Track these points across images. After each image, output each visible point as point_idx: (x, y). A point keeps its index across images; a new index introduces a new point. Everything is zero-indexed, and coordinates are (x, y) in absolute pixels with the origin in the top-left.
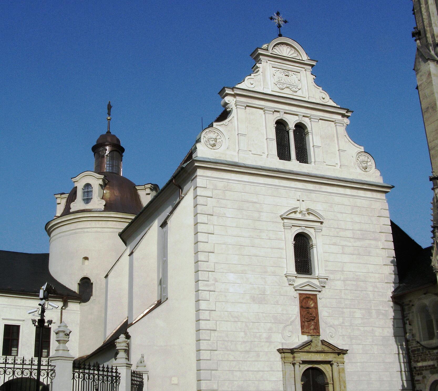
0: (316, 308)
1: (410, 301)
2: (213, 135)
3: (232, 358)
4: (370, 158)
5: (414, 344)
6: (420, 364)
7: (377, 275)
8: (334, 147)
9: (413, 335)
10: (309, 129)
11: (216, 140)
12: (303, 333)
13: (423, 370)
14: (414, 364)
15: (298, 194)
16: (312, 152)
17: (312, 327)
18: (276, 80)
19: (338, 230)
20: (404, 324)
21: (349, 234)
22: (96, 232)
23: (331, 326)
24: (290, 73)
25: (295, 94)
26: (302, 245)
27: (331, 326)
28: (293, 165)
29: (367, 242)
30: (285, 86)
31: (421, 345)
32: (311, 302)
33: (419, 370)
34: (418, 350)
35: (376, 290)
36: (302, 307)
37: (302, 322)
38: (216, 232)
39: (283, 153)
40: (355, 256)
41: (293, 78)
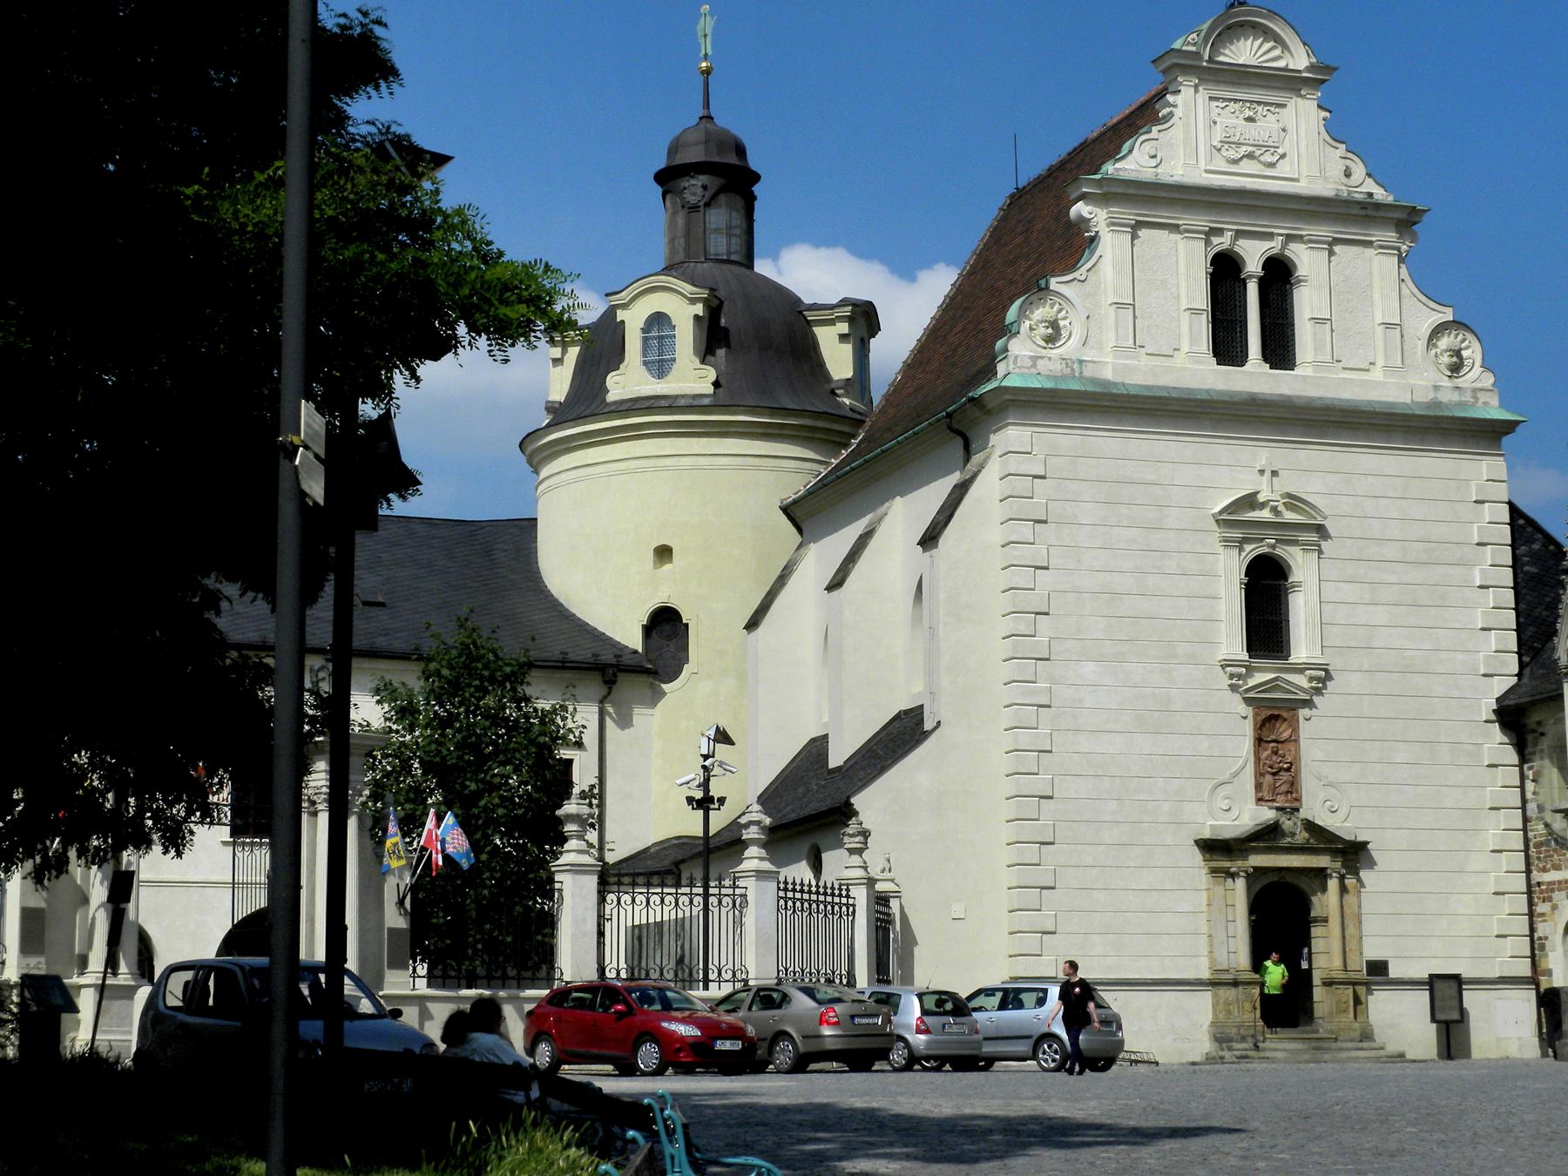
1: (1539, 723)
3: (1089, 861)
4: (1469, 336)
7: (1460, 656)
8: (1366, 323)
9: (1541, 808)
10: (1302, 270)
11: (1054, 324)
12: (1259, 800)
13: (1553, 890)
14: (1537, 876)
17: (1284, 788)
18: (1218, 134)
19: (1362, 543)
20: (1523, 777)
21: (1390, 551)
22: (694, 468)
25: (1269, 172)
27: (1330, 785)
28: (1254, 376)
30: (1243, 150)
32: (1285, 725)
33: (1547, 891)
35: (1456, 693)
36: (1259, 741)
37: (1259, 775)
38: (1053, 562)
39: (1227, 348)
41: (1268, 124)
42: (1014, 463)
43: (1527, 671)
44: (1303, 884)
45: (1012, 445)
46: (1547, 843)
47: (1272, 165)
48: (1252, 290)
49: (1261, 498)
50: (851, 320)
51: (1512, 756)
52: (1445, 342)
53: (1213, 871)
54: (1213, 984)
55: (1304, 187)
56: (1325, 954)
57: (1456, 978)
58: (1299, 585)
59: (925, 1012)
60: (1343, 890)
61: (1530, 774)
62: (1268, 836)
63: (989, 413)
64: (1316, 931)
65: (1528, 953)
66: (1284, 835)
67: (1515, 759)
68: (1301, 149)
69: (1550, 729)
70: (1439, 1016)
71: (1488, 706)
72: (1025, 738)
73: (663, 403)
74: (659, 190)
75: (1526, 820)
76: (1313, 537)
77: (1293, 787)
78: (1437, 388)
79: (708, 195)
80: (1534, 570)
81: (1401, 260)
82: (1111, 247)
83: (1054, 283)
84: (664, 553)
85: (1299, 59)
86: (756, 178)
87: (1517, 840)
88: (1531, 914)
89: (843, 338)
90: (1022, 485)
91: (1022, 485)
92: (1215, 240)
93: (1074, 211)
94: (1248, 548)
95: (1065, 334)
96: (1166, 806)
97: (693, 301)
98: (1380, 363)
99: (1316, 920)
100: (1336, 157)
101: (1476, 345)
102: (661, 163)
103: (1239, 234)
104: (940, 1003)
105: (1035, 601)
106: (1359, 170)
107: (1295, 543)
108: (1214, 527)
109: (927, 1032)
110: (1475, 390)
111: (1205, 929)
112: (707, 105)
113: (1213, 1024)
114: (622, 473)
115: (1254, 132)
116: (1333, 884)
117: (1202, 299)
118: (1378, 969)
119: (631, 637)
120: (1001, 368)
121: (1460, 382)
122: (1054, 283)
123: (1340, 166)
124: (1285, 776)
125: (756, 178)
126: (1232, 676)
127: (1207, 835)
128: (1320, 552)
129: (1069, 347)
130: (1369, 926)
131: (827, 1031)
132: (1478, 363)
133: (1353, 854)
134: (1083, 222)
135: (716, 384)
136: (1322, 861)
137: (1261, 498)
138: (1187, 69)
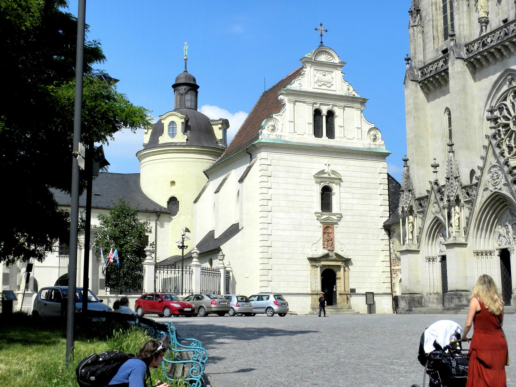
4: (378, 131)
6: (395, 268)
7: (375, 212)
9: (394, 251)
11: (274, 126)
17: (330, 245)
18: (316, 79)
20: (390, 243)
21: (358, 185)
25: (329, 89)
26: (326, 193)
28: (324, 141)
29: (370, 190)
30: (322, 83)
36: (324, 233)
37: (324, 241)
39: (317, 133)
40: (361, 200)
41: (328, 77)
42: (263, 162)
43: (391, 216)
44: (335, 269)
45: (262, 155)
46: (395, 259)
47: (330, 87)
48: (324, 119)
49: (325, 171)
50: (222, 124)
51: (387, 237)
52: (372, 133)
53: (312, 266)
54: (312, 294)
55: (337, 93)
56: (340, 287)
57: (372, 293)
59: (238, 301)
60: (345, 271)
61: (391, 242)
62: (326, 257)
64: (337, 281)
66: (330, 257)
67: (387, 238)
68: (337, 83)
69: (397, 231)
70: (368, 303)
73: (173, 144)
74: (173, 90)
75: (390, 253)
76: (338, 181)
77: (332, 245)
78: (370, 144)
79: (187, 90)
80: (393, 190)
81: (361, 112)
82: (289, 106)
83: (274, 116)
84: (173, 183)
85: (337, 61)
86: (198, 87)
88: (391, 277)
89: (220, 128)
90: (265, 167)
91: (265, 167)
92: (315, 106)
93: (279, 98)
94: (322, 184)
95: (277, 128)
96: (300, 249)
97: (181, 118)
99: (338, 278)
100: (345, 86)
101: (380, 134)
102: (174, 83)
103: (321, 104)
104: (242, 299)
105: (268, 197)
106: (351, 89)
107: (334, 183)
108: (313, 178)
109: (239, 306)
110: (379, 145)
111: (310, 280)
112: (186, 68)
115: (325, 79)
116: (342, 269)
117: (311, 120)
118: (353, 291)
119: (164, 204)
120: (260, 137)
121: (375, 143)
122: (274, 116)
123: (347, 88)
124: (330, 242)
125: (198, 87)
126: (317, 216)
127: (311, 257)
128: (340, 185)
129: (278, 133)
131: (213, 306)
132: (380, 138)
133: (347, 262)
134: (282, 100)
135: (187, 140)
136: (339, 263)
137: (325, 171)
138: (308, 62)
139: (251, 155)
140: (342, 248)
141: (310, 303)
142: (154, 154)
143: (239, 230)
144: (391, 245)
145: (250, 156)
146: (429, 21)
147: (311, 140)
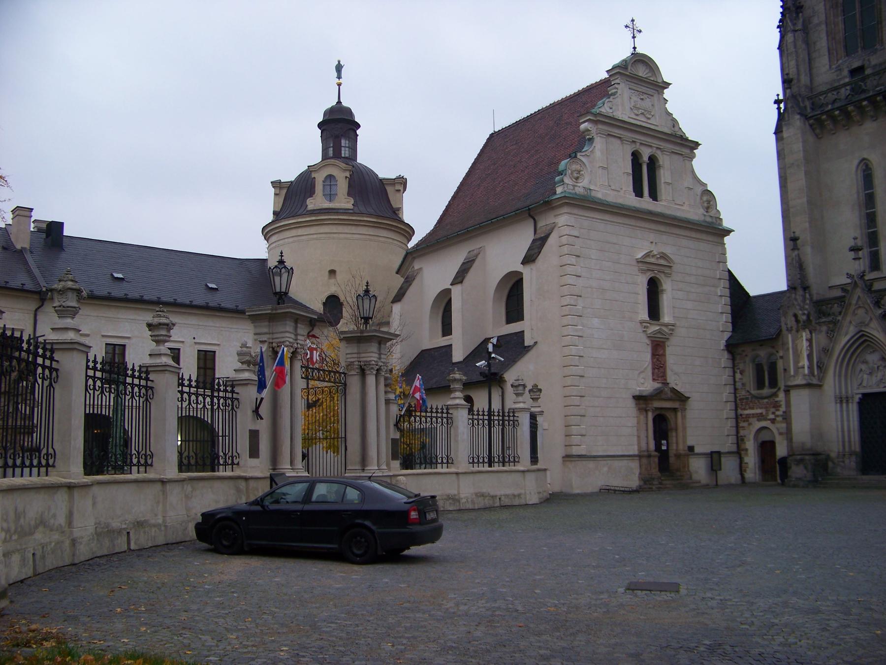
0: (664, 355)
2: (578, 167)
5: (743, 393)
6: (746, 412)
9: (743, 384)
11: (579, 172)
12: (654, 380)
15: (652, 236)
16: (664, 191)
18: (633, 104)
20: (734, 372)
23: (676, 374)
24: (645, 96)
26: (654, 290)
27: (676, 374)
31: (751, 394)
34: (747, 398)
37: (653, 369)
41: (647, 103)
45: (563, 221)
47: (649, 119)
54: (640, 456)
56: (676, 445)
58: (662, 290)
62: (657, 395)
63: (553, 208)
65: (735, 442)
71: (723, 343)
72: (573, 350)
75: (735, 389)
77: (664, 376)
86: (358, 126)
87: (732, 398)
88: (737, 427)
93: (583, 127)
98: (687, 203)
113: (640, 474)
114: (316, 239)
116: (679, 414)
118: (691, 449)
119: (318, 307)
124: (662, 370)
125: (358, 126)
127: (637, 394)
129: (584, 183)
130: (689, 432)
139: (534, 219)
140: (677, 380)
141: (637, 472)
142: (299, 225)
143: (528, 349)
144: (738, 376)
145: (532, 221)
146: (819, 24)
147: (629, 199)
